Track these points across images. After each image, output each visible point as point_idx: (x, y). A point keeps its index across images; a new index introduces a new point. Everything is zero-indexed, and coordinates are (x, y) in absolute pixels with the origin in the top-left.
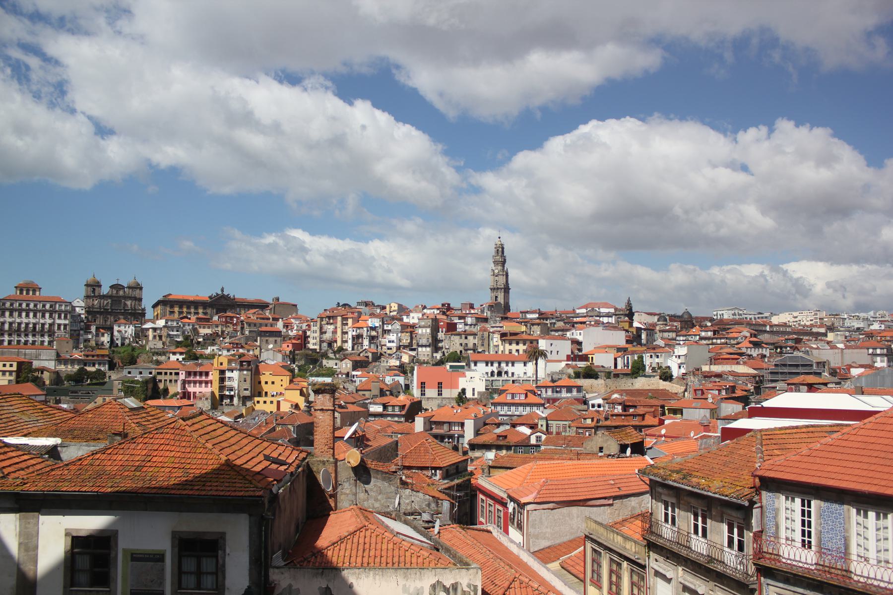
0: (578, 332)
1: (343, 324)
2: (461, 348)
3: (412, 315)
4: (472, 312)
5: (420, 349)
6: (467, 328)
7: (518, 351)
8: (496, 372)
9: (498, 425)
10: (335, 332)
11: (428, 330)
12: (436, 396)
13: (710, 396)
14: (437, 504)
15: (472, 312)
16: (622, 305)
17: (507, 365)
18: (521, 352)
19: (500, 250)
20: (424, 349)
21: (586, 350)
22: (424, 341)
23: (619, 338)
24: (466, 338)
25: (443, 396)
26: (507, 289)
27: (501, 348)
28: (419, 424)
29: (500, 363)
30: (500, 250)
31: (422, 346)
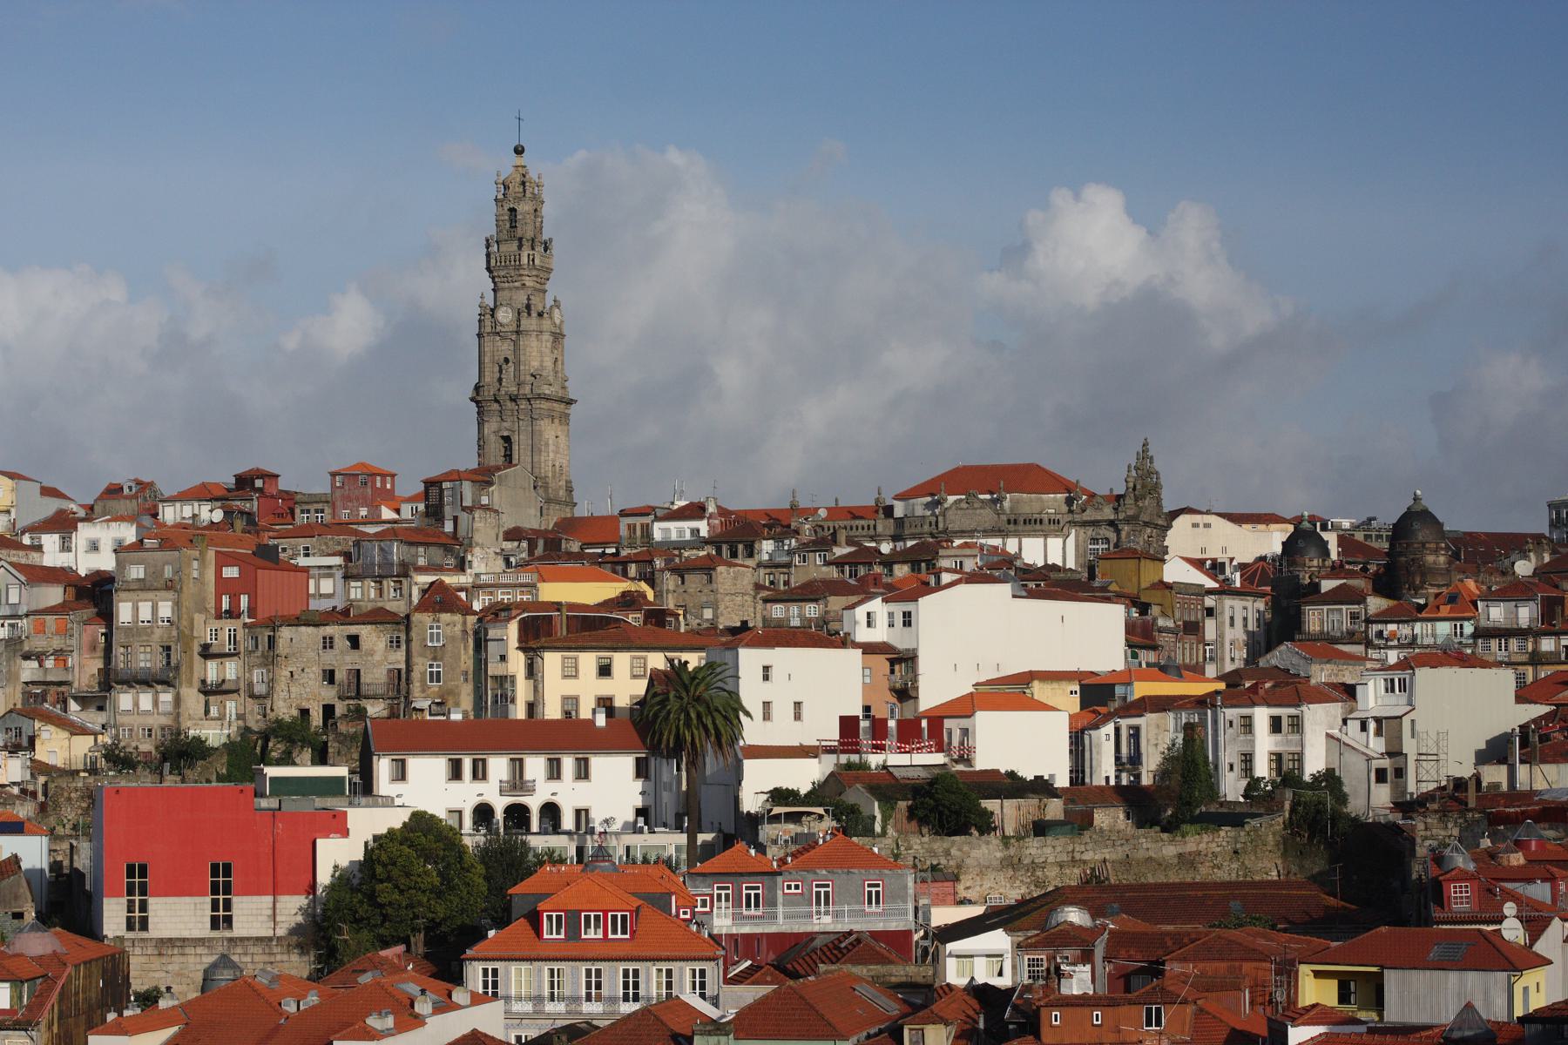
0: (898, 609)
2: (329, 694)
3: (85, 533)
4: (387, 514)
5: (125, 700)
6: (356, 591)
8: (499, 804)
11: (166, 610)
12: (202, 929)
13: (1510, 908)
15: (387, 514)
17: (554, 773)
20: (146, 701)
21: (931, 696)
22: (146, 659)
24: (354, 641)
25: (241, 928)
27: (523, 691)
29: (518, 767)
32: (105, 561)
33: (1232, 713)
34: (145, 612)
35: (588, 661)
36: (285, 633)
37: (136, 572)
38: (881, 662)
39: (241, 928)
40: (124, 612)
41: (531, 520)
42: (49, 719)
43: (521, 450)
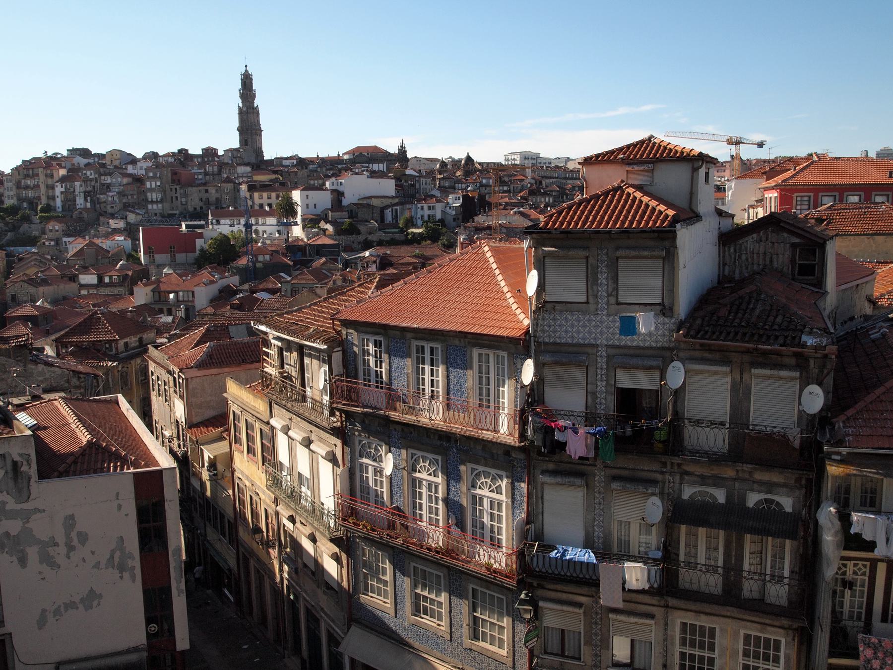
1: (46, 175)
2: (201, 204)
5: (150, 207)
7: (270, 205)
9: (237, 292)
10: (37, 186)
11: (158, 183)
14: (79, 378)
15: (216, 159)
16: (393, 149)
18: (274, 207)
19: (247, 81)
20: (155, 206)
22: (154, 196)
23: (388, 187)
24: (207, 191)
25: (178, 261)
26: (258, 132)
27: (250, 203)
28: (142, 295)
30: (247, 81)
31: (152, 202)
32: (143, 172)
33: (419, 205)
34: (153, 183)
35: (265, 195)
36: (190, 189)
37: (151, 174)
38: (336, 194)
39: (178, 261)
40: (148, 185)
41: (253, 160)
42: (130, 211)
43: (249, 143)
